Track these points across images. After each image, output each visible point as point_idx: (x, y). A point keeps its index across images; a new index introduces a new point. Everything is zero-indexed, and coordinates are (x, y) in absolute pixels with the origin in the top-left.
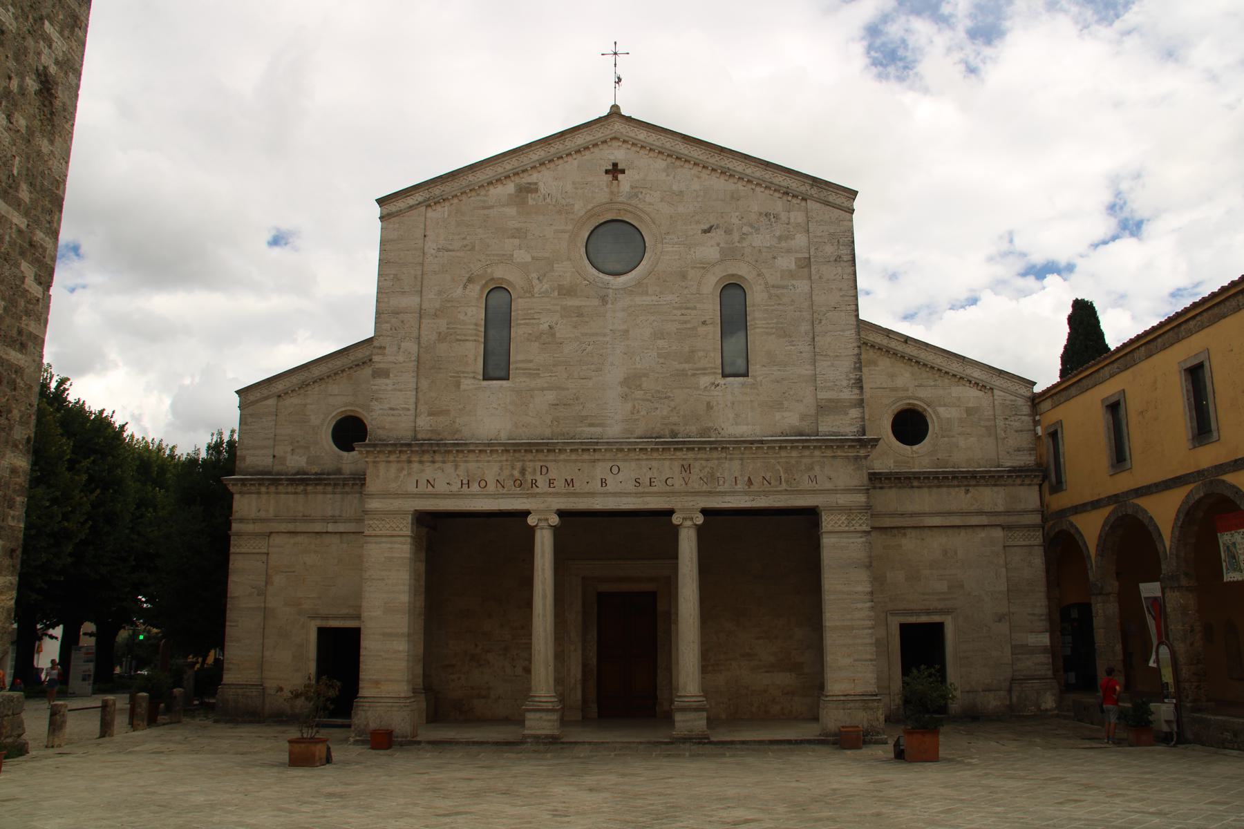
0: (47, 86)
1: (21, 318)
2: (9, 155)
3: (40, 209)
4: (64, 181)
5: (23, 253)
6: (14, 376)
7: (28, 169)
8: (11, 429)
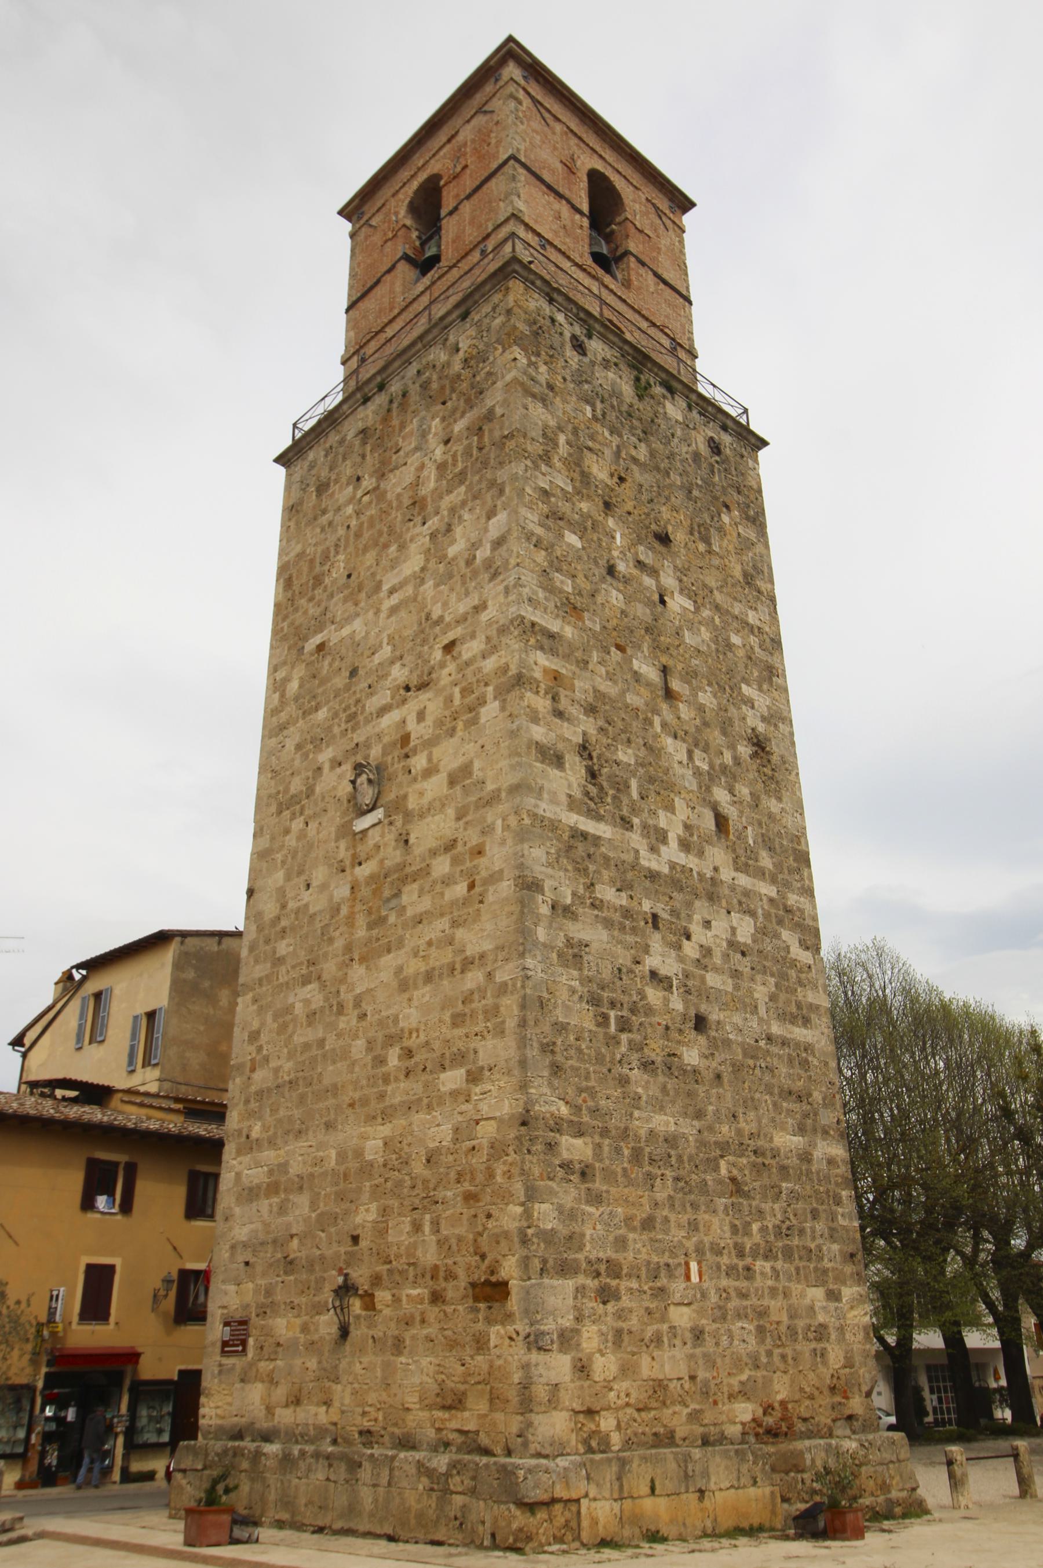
0: (760, 746)
1: (796, 990)
2: (740, 828)
3: (786, 872)
4: (804, 834)
5: (780, 922)
6: (804, 1055)
7: (763, 835)
8: (816, 1114)
